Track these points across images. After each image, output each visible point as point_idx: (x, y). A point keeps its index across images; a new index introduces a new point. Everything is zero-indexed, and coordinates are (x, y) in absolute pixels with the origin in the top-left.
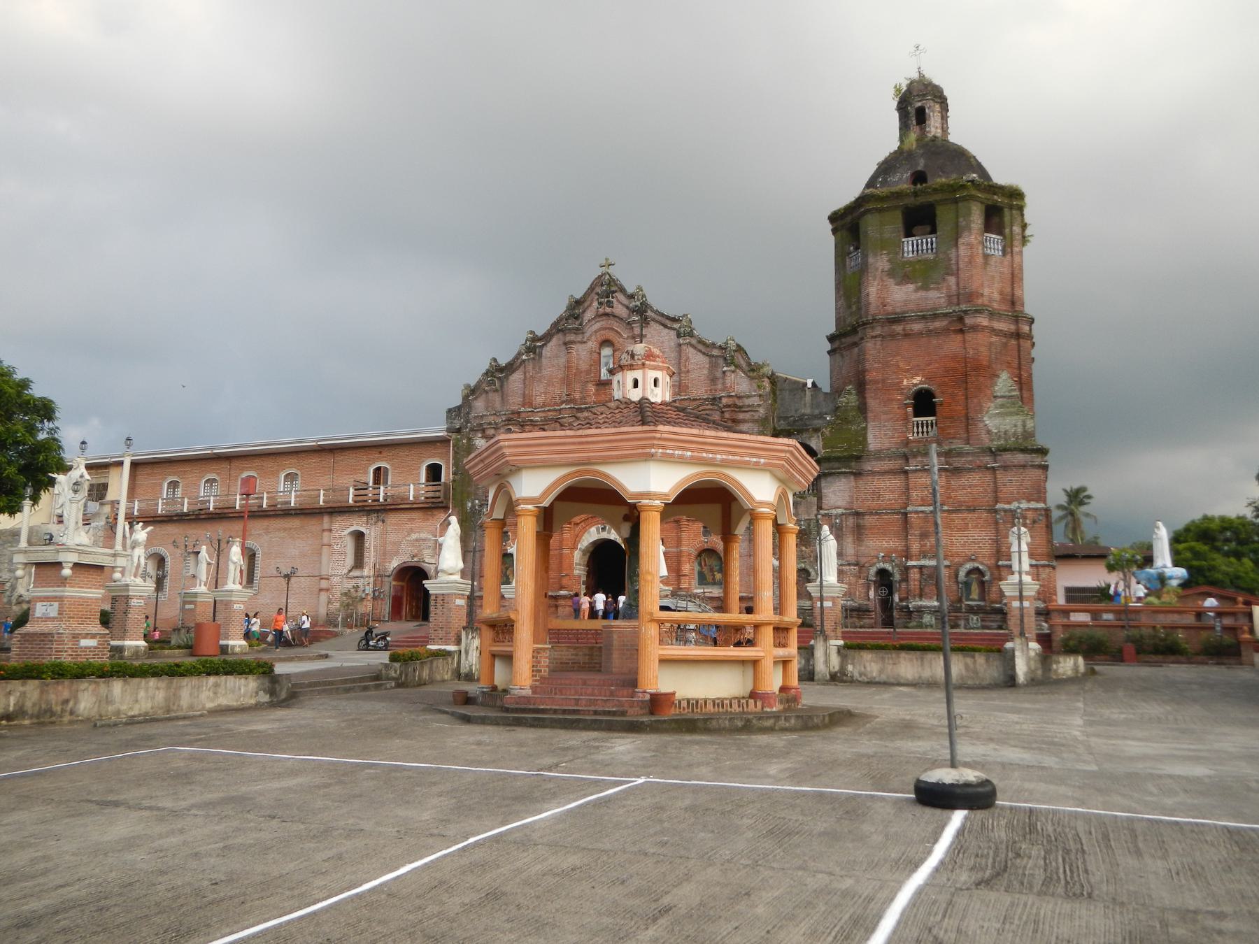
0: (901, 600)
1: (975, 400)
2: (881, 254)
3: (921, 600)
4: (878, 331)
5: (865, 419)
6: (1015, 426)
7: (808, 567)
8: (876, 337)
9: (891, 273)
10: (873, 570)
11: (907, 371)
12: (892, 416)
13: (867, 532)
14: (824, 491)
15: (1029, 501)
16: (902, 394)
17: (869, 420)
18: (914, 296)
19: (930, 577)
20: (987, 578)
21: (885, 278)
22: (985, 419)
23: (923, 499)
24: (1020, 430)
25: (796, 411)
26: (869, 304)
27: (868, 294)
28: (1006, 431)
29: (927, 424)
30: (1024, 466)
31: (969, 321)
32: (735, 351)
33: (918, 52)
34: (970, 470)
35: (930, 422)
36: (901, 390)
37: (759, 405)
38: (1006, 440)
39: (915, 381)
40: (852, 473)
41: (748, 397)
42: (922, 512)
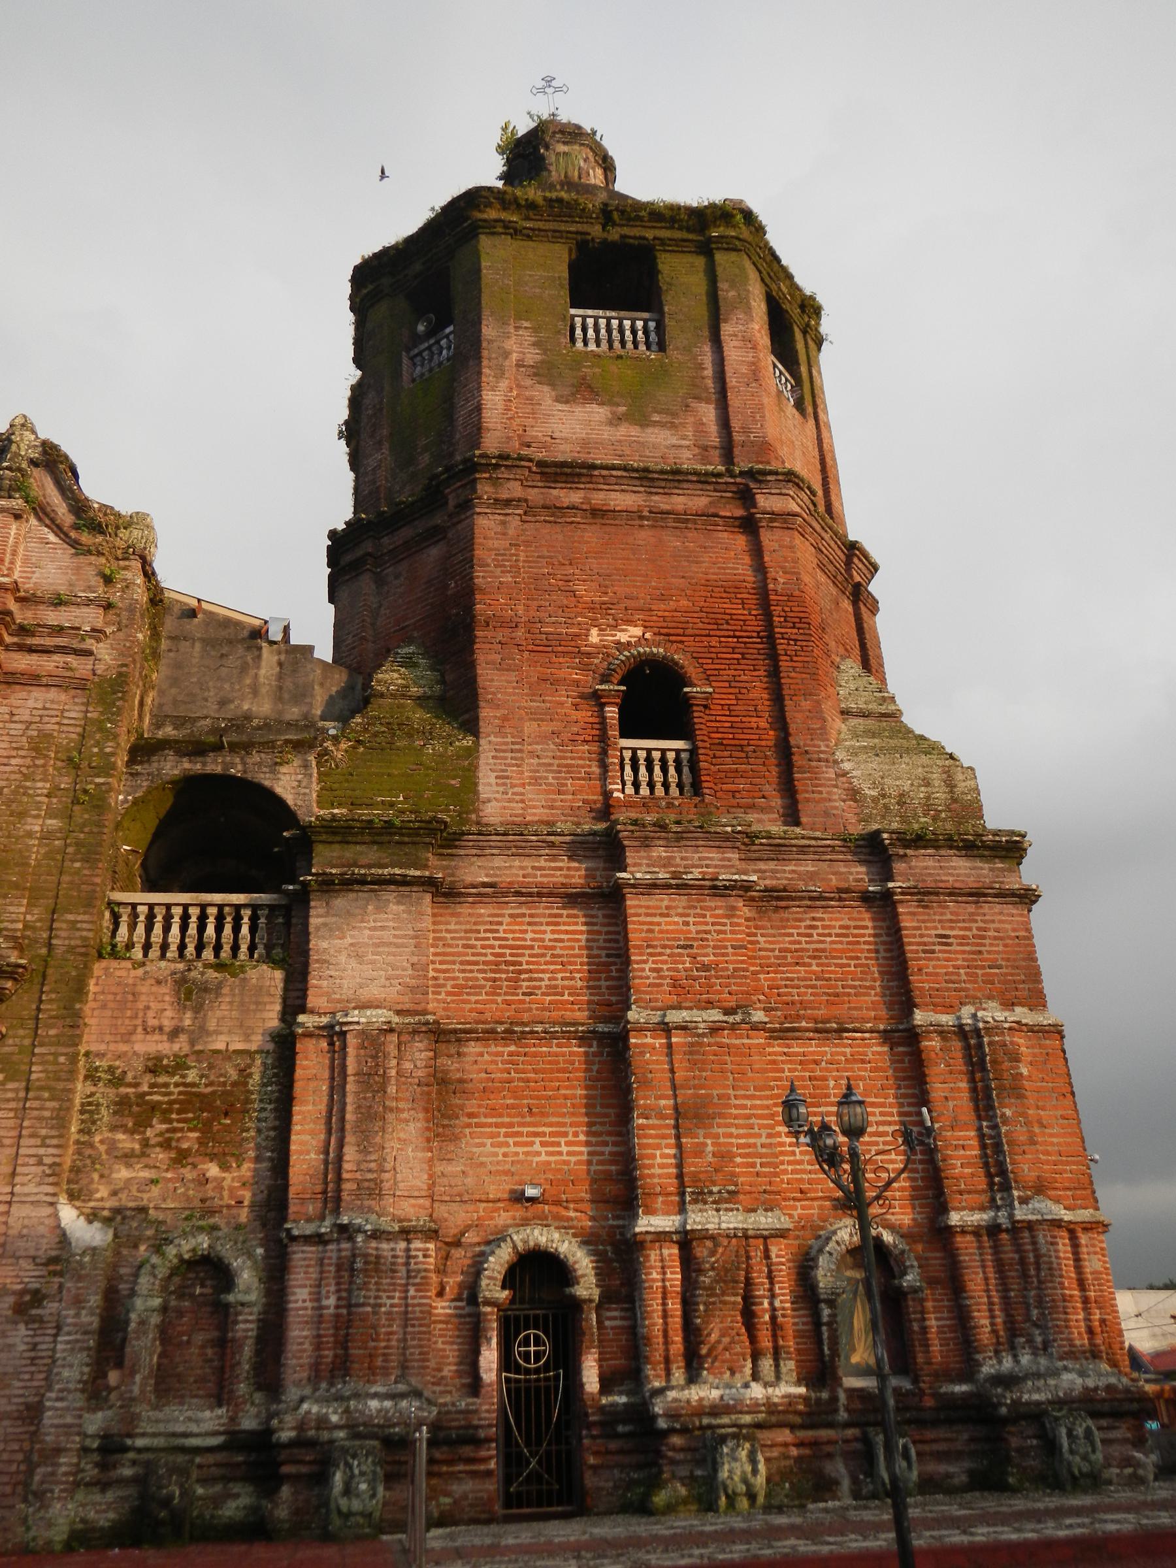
0: (607, 1384)
1: (806, 704)
2: (517, 328)
3: (693, 1378)
4: (514, 489)
5: (471, 727)
6: (928, 785)
7: (226, 1250)
8: (508, 503)
9: (544, 373)
10: (499, 1261)
11: (605, 608)
12: (555, 726)
13: (472, 1105)
14: (319, 944)
15: (1009, 1005)
16: (585, 667)
17: (484, 727)
18: (607, 433)
19: (726, 1277)
20: (911, 1279)
21: (528, 382)
22: (840, 755)
23: (675, 984)
24: (940, 795)
25: (223, 703)
26: (477, 430)
27: (479, 409)
28: (902, 795)
29: (663, 760)
30: (977, 895)
31: (766, 502)
32: (33, 463)
33: (550, 90)
34: (817, 900)
35: (671, 756)
36: (584, 656)
37: (97, 633)
38: (904, 819)
39: (623, 637)
40: (430, 884)
41: (58, 602)
42: (683, 1028)
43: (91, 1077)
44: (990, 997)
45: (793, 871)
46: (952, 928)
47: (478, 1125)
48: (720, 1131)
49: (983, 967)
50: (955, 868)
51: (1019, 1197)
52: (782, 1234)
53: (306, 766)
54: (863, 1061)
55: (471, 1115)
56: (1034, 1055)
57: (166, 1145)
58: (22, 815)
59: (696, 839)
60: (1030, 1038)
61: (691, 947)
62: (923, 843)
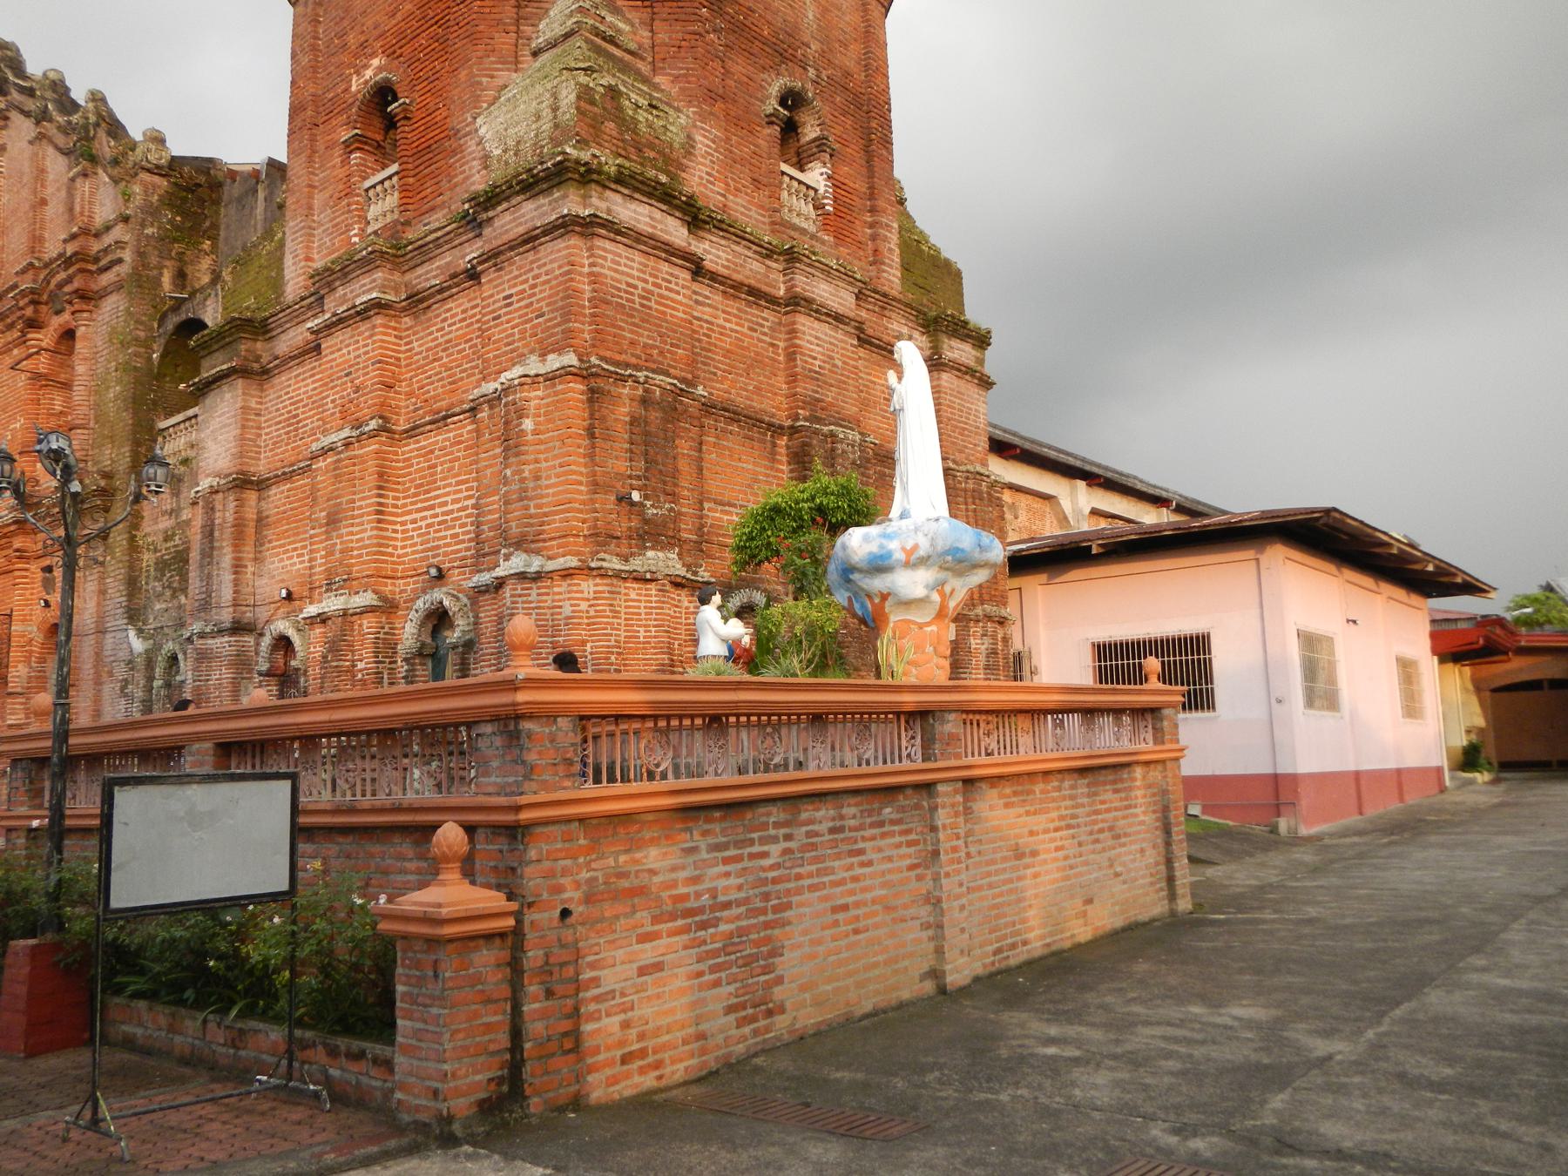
6: (538, 117)
30: (530, 240)
43: (148, 550)
44: (532, 352)
45: (438, 267)
46: (515, 285)
47: (273, 548)
48: (344, 531)
49: (531, 320)
50: (523, 216)
51: (505, 555)
52: (369, 610)
53: (217, 295)
54: (460, 443)
55: (270, 542)
56: (548, 405)
57: (169, 587)
58: (108, 388)
59: (353, 271)
60: (546, 387)
61: (350, 373)
62: (494, 201)
